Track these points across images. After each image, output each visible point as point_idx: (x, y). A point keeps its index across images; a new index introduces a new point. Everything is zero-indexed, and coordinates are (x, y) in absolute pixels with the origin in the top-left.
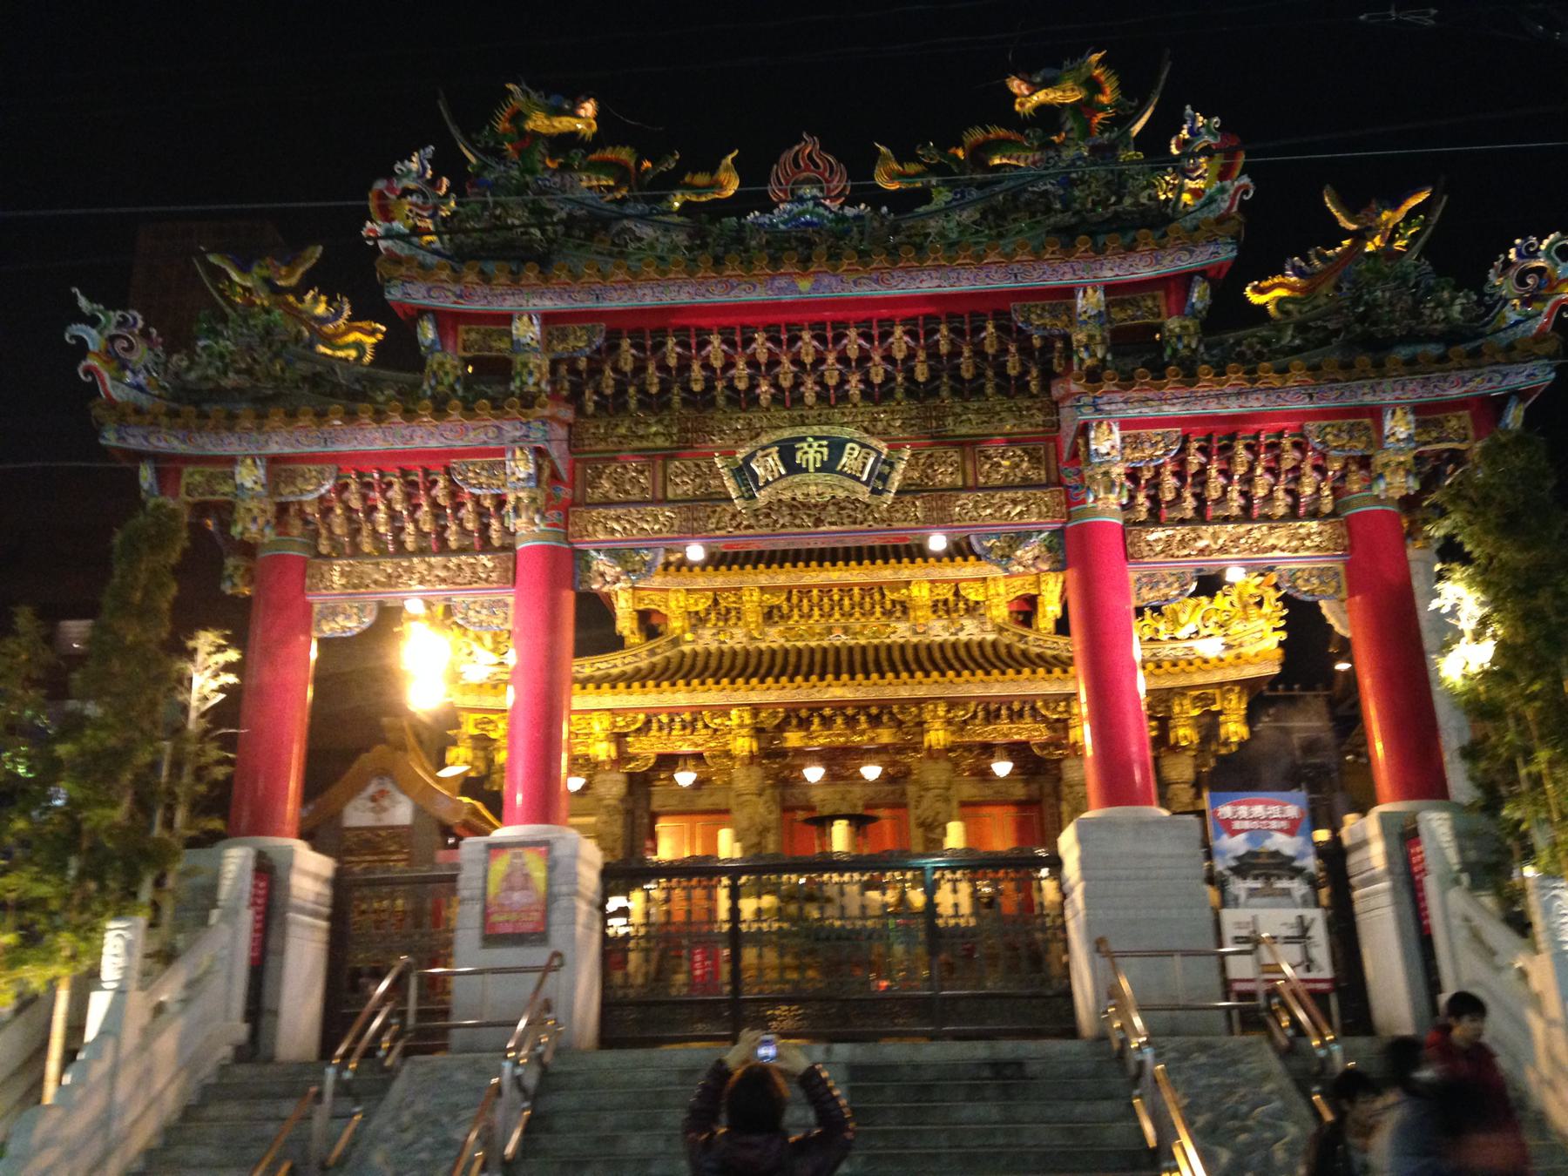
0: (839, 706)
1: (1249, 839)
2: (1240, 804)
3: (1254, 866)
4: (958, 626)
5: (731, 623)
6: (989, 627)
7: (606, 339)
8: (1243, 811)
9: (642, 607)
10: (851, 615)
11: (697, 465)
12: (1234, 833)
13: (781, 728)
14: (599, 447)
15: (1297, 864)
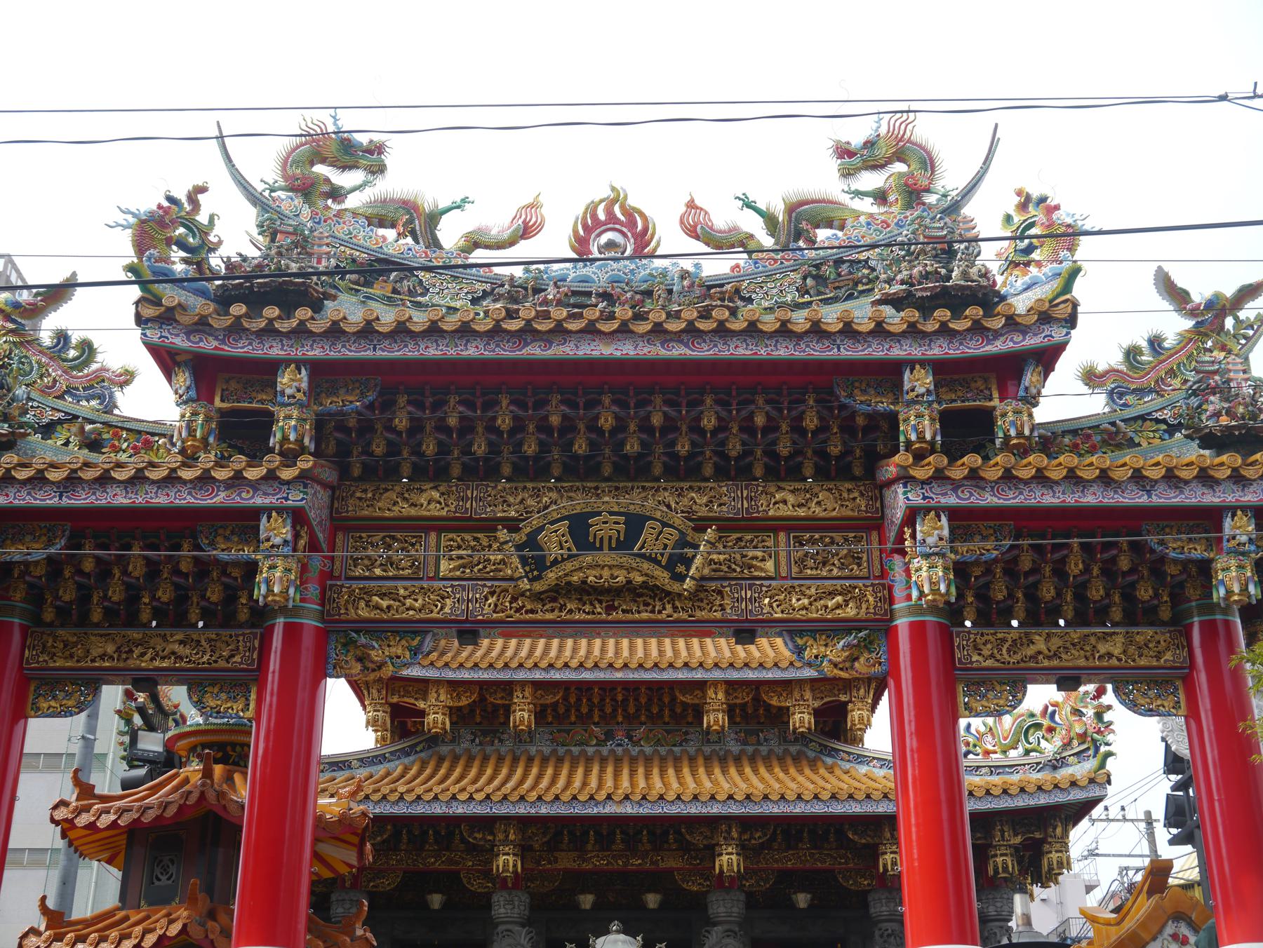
7: (381, 394)
11: (475, 539)
14: (365, 513)
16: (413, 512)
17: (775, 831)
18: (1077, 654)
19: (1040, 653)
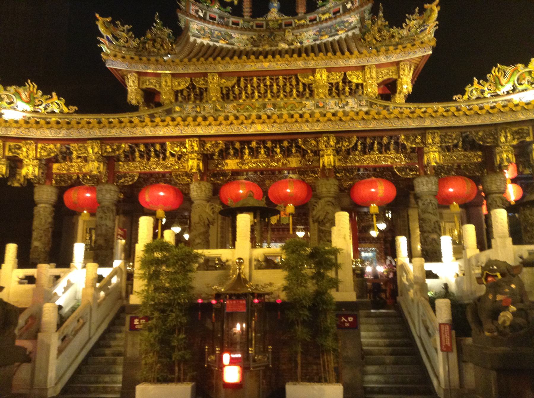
0: (262, 138)
4: (344, 103)
5: (204, 101)
6: (364, 103)
9: (144, 87)
10: (278, 97)
13: (224, 154)
17: (356, 145)
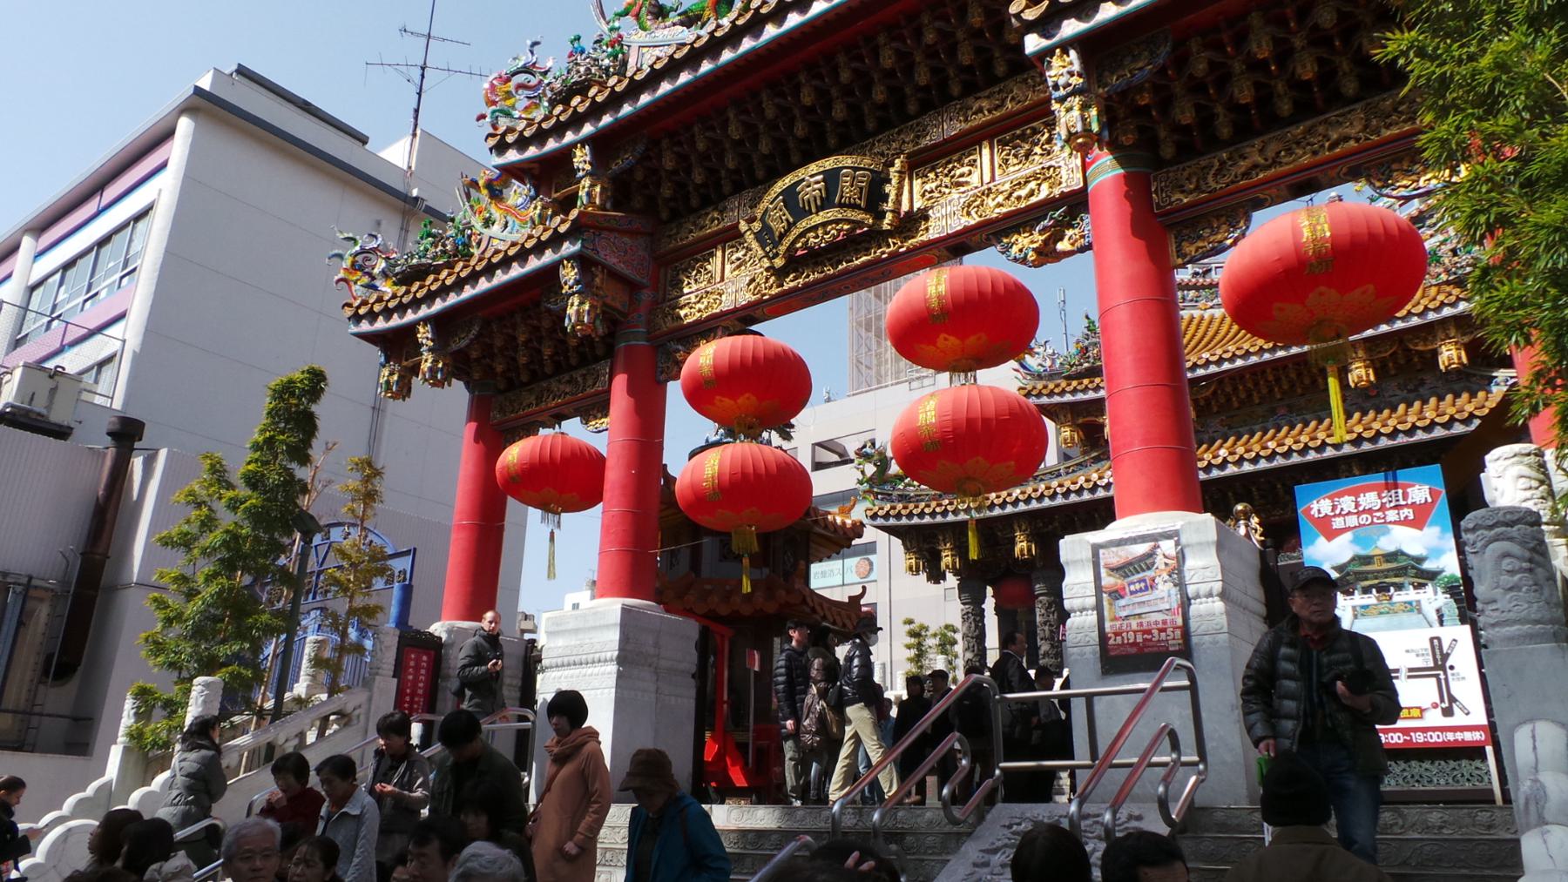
1: (1355, 541)
2: (1341, 495)
3: (1363, 576)
8: (1347, 503)
12: (1331, 534)
15: (1427, 566)
16: (702, 233)
18: (1300, 152)
19: (1255, 166)
